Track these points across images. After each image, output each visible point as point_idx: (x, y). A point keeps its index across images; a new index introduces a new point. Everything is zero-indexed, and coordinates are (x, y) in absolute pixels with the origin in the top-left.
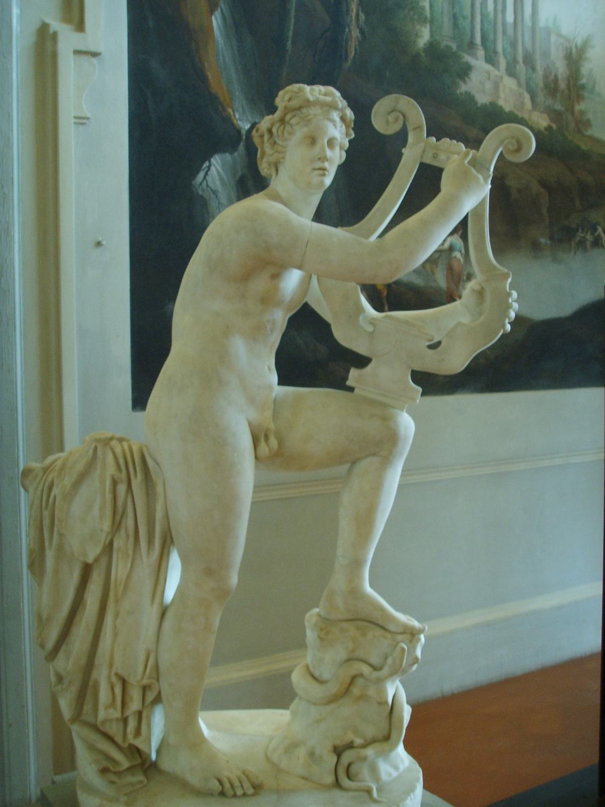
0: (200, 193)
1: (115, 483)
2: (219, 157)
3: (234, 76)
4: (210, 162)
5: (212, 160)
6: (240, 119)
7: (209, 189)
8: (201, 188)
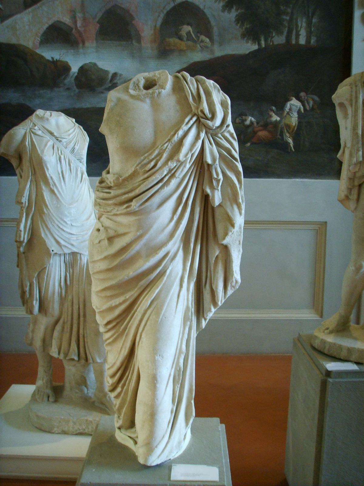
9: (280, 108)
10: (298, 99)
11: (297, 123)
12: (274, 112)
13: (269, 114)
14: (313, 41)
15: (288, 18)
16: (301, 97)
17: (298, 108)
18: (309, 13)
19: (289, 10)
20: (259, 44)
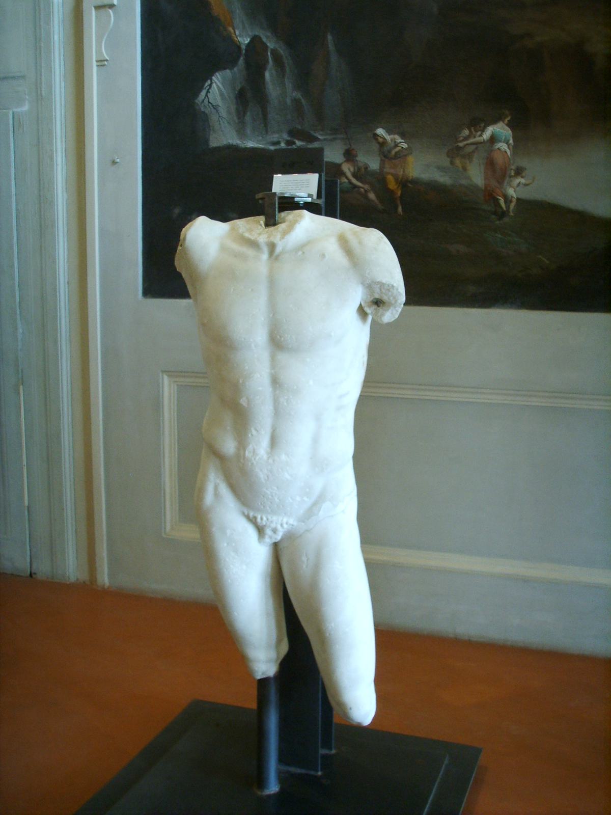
0: (202, 109)
2: (220, 74)
4: (211, 80)
6: (240, 35)
7: (210, 105)
8: (203, 105)
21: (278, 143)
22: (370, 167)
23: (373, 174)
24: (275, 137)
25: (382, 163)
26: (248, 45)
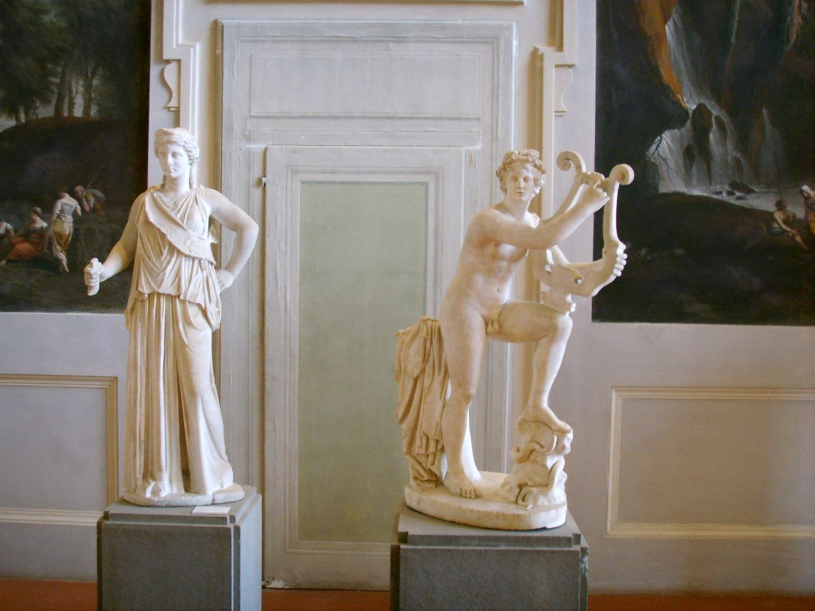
0: (653, 161)
1: (425, 340)
3: (683, 68)
4: (661, 136)
5: (663, 135)
6: (687, 102)
7: (660, 157)
8: (653, 157)
9: (48, 210)
10: (73, 195)
11: (72, 231)
12: (39, 215)
13: (31, 218)
14: (94, 112)
15: (57, 80)
16: (77, 193)
17: (74, 209)
18: (87, 72)
19: (59, 70)
20: (18, 119)
21: (720, 193)
22: (796, 216)
23: (800, 221)
24: (718, 188)
25: (807, 213)
26: (695, 111)
